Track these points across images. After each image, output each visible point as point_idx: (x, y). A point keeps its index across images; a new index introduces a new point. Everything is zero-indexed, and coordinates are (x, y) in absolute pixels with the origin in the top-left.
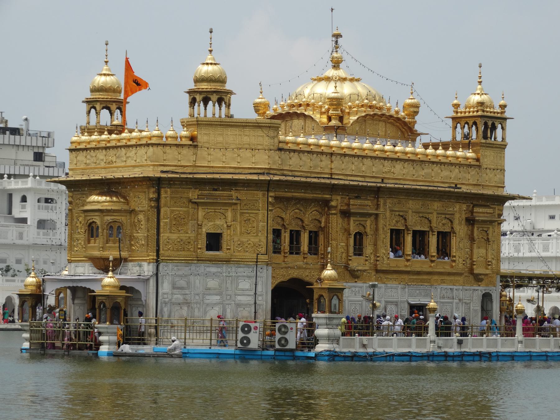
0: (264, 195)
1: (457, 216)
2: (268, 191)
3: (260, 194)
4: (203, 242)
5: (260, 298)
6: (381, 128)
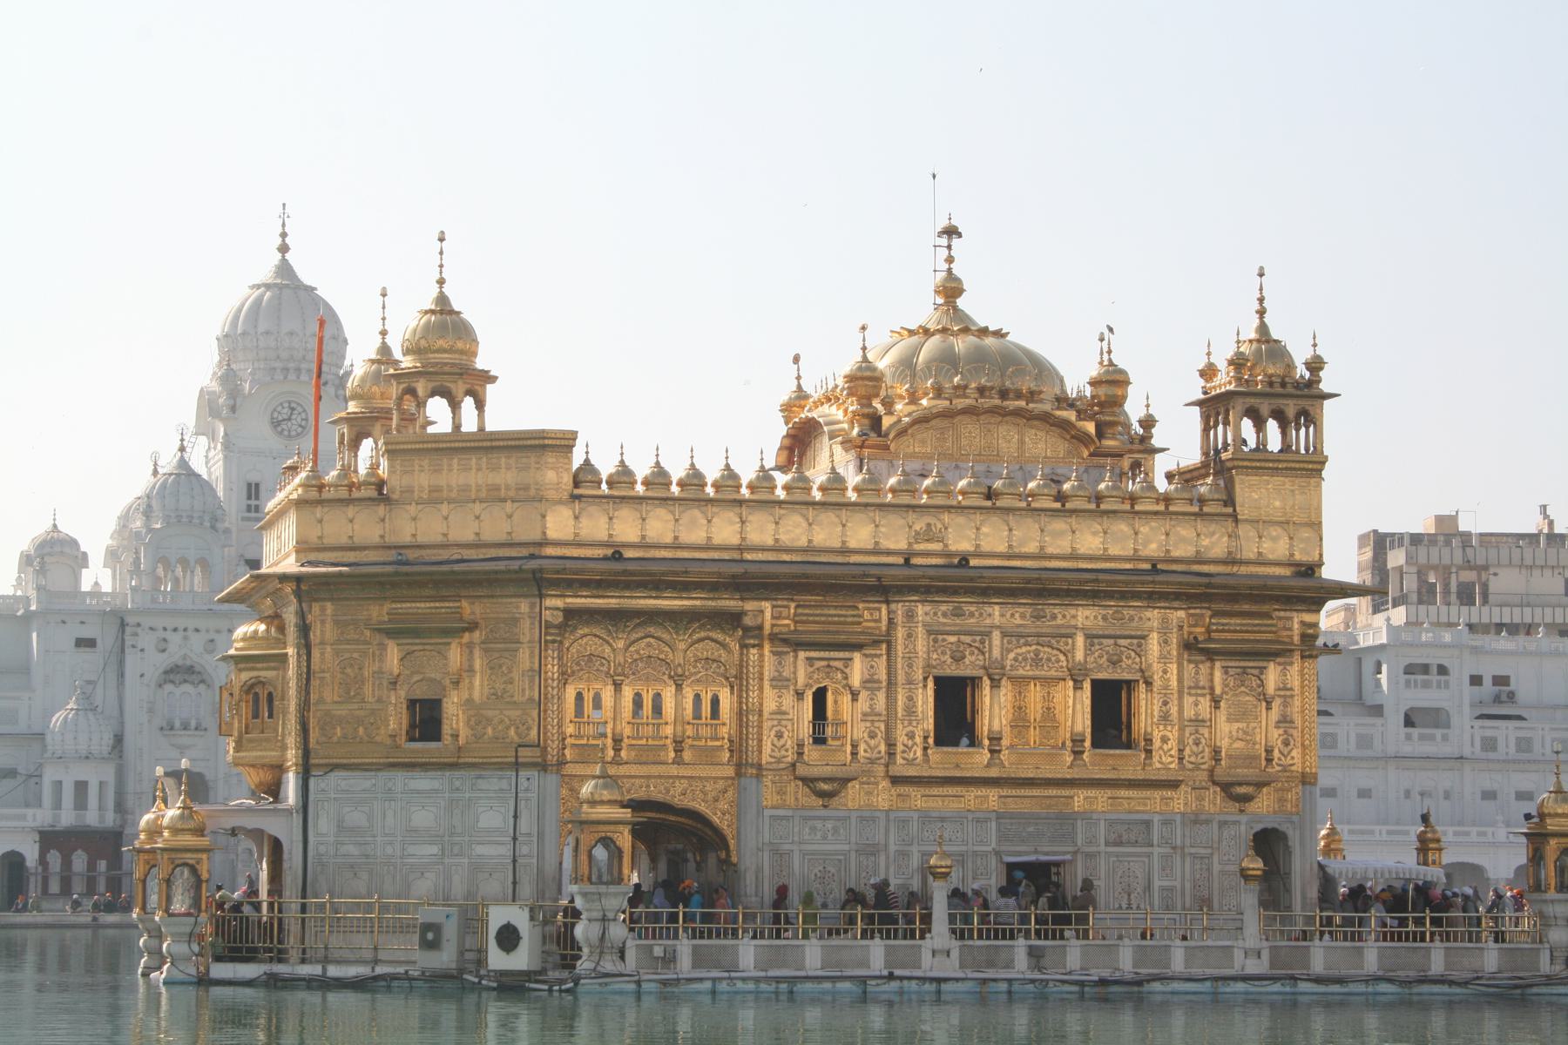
0: (532, 606)
1: (1154, 639)
2: (541, 596)
3: (524, 606)
4: (396, 720)
5: (525, 850)
6: (1007, 438)
